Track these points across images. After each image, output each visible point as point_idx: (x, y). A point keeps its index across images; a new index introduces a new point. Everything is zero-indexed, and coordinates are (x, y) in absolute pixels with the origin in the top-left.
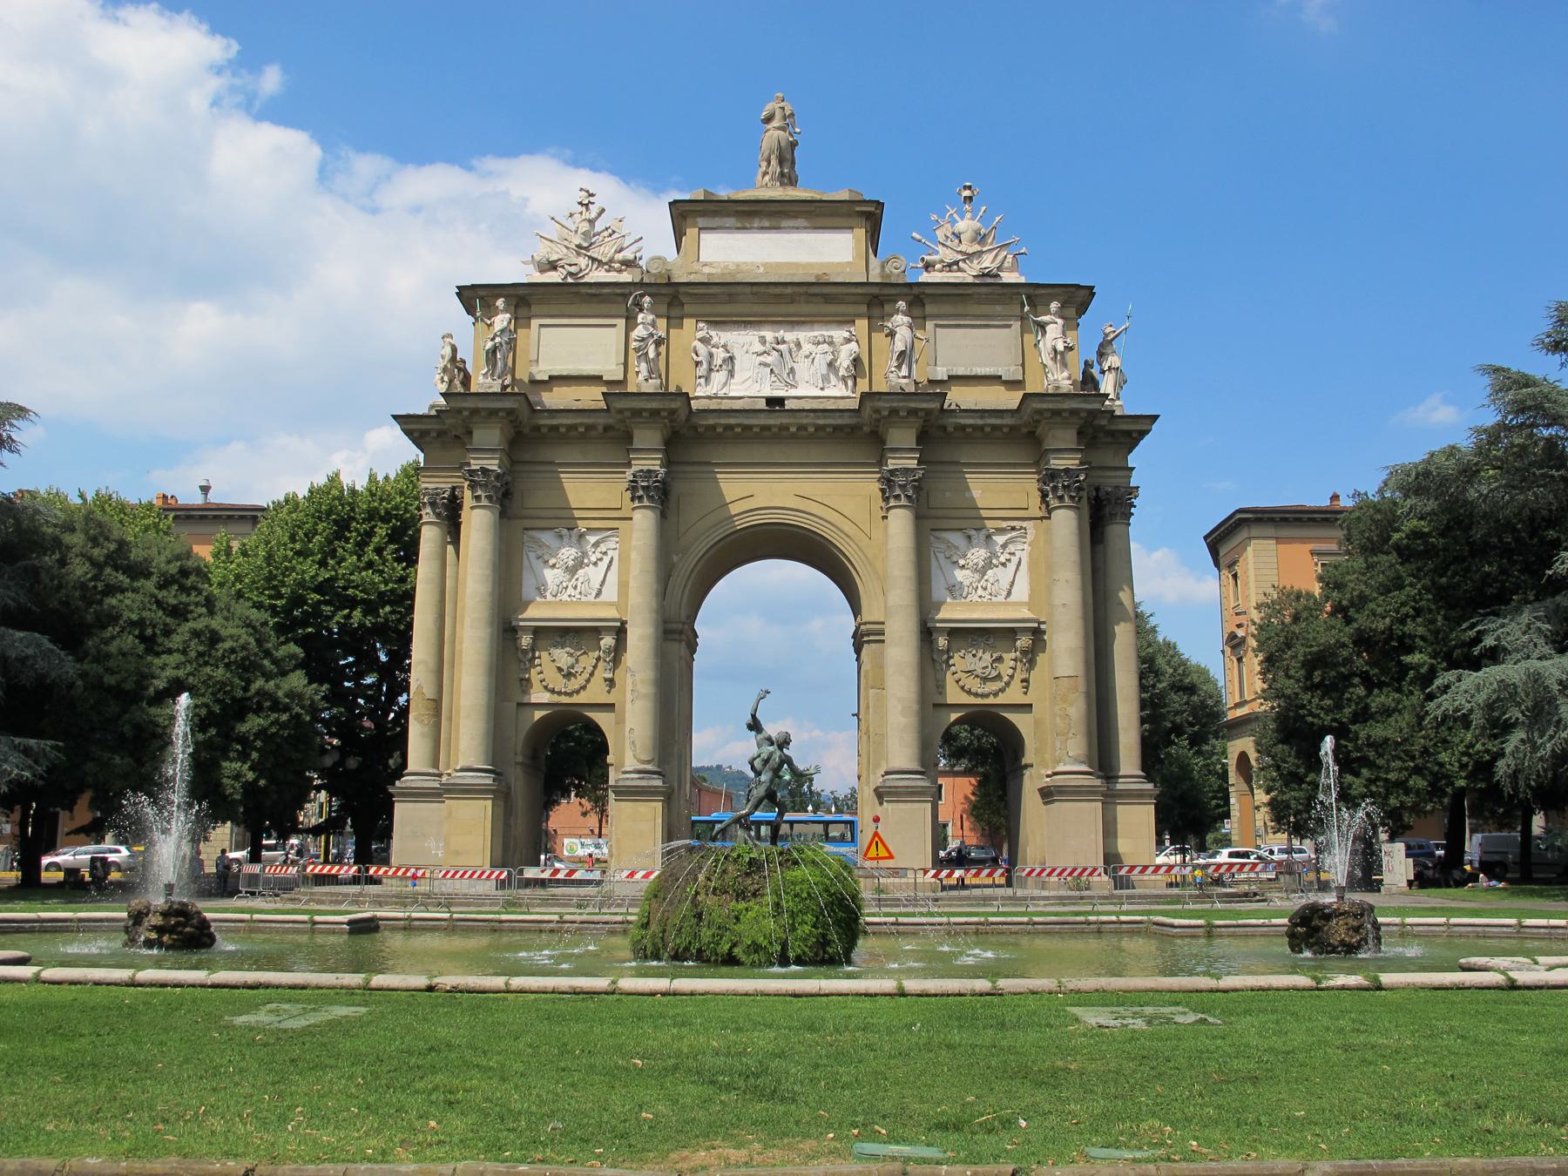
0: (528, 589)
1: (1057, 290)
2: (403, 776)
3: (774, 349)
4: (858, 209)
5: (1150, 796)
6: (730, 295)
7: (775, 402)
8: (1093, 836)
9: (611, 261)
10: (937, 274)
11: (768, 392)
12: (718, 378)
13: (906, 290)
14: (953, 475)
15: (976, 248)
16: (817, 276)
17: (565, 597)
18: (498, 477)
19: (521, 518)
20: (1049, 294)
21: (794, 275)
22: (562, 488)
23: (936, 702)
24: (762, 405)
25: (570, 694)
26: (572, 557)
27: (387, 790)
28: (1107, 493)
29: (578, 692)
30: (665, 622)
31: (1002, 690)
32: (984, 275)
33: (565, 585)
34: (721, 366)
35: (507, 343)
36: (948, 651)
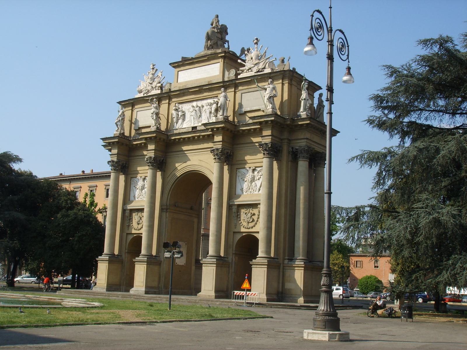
0: (238, 191)
1: (278, 74)
2: (103, 255)
3: (194, 110)
4: (219, 55)
5: (302, 267)
6: (183, 93)
7: (194, 128)
8: (263, 281)
9: (156, 87)
10: (245, 74)
11: (193, 125)
12: (180, 121)
13: (231, 83)
14: (174, 156)
15: (257, 61)
16: (209, 82)
17: (140, 199)
18: (116, 162)
19: (236, 164)
20: (276, 76)
21: (202, 83)
22: (189, 158)
23: (234, 231)
24: (190, 130)
25: (139, 230)
26: (141, 186)
27: (96, 259)
28: (296, 149)
29: (252, 228)
30: (162, 206)
31: (254, 226)
32: (258, 72)
33: (139, 195)
34: (180, 118)
35: (122, 120)
36: (238, 212)
